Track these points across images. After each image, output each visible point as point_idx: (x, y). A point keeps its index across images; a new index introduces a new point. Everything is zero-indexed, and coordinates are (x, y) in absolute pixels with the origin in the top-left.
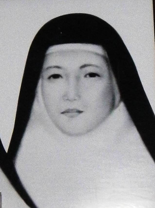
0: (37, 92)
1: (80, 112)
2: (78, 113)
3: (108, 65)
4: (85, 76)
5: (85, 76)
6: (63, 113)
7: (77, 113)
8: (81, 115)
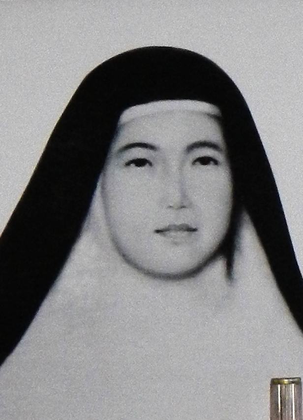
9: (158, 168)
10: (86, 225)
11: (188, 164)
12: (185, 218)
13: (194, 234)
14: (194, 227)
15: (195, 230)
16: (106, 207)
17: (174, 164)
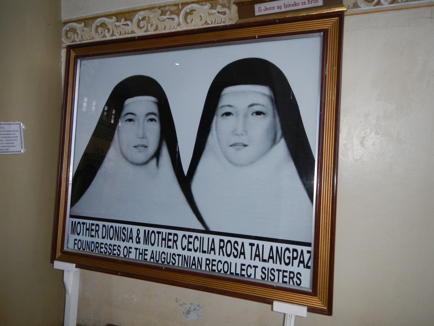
0: (212, 127)
1: (245, 146)
2: (243, 146)
3: (273, 105)
4: (252, 114)
5: (252, 114)
6: (231, 146)
7: (242, 147)
8: (246, 148)
9: (136, 123)
10: (112, 143)
12: (144, 142)
13: (147, 148)
14: (146, 145)
15: (147, 147)
16: (119, 137)
17: (141, 121)
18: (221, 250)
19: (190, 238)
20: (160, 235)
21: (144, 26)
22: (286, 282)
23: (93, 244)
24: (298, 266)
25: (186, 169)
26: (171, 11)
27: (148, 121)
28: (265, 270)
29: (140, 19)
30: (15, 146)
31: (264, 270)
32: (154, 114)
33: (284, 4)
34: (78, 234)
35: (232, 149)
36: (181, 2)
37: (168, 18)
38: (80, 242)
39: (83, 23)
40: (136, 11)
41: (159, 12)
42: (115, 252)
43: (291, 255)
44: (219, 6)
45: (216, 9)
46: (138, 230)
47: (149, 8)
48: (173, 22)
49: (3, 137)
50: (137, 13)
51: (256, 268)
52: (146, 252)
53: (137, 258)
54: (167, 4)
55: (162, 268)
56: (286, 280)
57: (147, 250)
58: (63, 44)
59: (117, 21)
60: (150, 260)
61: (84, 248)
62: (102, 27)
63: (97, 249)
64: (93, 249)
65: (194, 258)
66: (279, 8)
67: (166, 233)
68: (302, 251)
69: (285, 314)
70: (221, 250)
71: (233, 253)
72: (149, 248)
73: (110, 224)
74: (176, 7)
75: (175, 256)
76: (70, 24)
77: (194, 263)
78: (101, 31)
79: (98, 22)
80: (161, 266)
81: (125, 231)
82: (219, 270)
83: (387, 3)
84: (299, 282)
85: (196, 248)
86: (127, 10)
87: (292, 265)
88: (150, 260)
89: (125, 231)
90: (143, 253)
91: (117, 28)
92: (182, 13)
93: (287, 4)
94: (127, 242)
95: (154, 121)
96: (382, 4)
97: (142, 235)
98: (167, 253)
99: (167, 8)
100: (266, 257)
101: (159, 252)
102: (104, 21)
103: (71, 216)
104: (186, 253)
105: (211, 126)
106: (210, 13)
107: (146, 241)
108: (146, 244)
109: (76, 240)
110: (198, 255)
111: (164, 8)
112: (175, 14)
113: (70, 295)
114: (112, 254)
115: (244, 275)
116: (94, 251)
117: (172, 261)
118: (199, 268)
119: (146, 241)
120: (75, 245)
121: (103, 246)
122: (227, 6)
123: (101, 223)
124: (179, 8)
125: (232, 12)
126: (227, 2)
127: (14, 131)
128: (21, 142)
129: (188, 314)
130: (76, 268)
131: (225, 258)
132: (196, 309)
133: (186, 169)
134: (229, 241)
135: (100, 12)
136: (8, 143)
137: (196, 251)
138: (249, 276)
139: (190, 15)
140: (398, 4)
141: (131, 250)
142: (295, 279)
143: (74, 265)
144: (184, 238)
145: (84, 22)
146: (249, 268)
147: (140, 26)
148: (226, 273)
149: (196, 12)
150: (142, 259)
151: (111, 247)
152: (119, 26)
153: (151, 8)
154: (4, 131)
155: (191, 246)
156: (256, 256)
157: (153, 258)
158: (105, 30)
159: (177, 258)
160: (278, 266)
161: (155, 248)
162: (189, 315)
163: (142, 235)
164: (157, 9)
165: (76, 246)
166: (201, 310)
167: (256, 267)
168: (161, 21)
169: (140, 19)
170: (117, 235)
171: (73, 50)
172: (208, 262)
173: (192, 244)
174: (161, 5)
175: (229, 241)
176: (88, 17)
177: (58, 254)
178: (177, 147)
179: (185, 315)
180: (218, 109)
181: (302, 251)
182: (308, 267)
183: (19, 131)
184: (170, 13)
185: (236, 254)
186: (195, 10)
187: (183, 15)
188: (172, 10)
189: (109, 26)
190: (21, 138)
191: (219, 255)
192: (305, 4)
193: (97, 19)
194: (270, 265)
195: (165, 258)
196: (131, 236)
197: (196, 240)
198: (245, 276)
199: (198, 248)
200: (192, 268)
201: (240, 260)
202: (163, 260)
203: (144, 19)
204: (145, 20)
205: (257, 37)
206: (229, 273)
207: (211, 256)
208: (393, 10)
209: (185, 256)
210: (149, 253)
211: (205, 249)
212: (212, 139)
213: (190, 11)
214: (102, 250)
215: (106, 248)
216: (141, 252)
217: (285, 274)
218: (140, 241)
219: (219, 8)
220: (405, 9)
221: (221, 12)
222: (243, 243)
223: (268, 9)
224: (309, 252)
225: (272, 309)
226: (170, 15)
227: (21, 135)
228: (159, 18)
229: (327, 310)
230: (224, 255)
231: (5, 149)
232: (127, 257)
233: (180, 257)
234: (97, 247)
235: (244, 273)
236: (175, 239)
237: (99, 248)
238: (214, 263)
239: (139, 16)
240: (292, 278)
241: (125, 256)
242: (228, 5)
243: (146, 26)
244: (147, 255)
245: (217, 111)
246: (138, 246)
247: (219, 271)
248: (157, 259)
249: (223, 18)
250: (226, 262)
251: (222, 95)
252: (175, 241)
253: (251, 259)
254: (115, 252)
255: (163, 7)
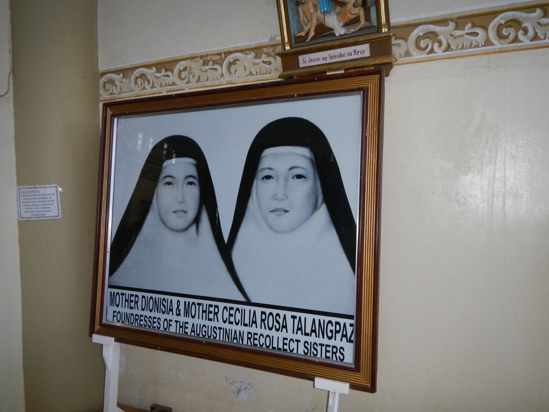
0: (252, 191)
1: (286, 211)
2: (284, 212)
3: (314, 168)
4: (293, 178)
6: (272, 211)
9: (175, 185)
11: (185, 184)
12: (183, 207)
13: (186, 214)
14: (186, 210)
17: (180, 184)
18: (263, 323)
19: (231, 311)
20: (201, 307)
21: (186, 77)
22: (329, 358)
23: (132, 316)
24: (341, 340)
25: (226, 235)
26: (213, 61)
27: (187, 184)
28: (308, 344)
29: (182, 70)
30: (51, 211)
31: (306, 344)
32: (194, 177)
33: (329, 55)
34: (117, 306)
35: (272, 215)
36: (224, 51)
37: (211, 69)
38: (119, 314)
39: (122, 74)
40: (177, 61)
41: (201, 61)
42: (155, 325)
43: (333, 328)
44: (264, 54)
45: (260, 58)
46: (179, 301)
47: (191, 57)
48: (215, 72)
49: (39, 202)
50: (178, 64)
51: (299, 343)
52: (187, 325)
53: (178, 332)
54: (209, 53)
55: (203, 342)
56: (329, 355)
57: (187, 323)
58: (101, 97)
59: (157, 72)
60: (191, 334)
61: (123, 320)
62: (141, 78)
63: (136, 321)
64: (132, 322)
65: (236, 331)
66: (324, 60)
67: (207, 305)
68: (345, 324)
69: (329, 392)
70: (263, 323)
71: (275, 326)
72: (190, 320)
73: (149, 295)
74: (219, 56)
75: (216, 330)
76: (108, 75)
77: (235, 337)
78: (141, 83)
79: (137, 73)
80: (202, 340)
81: (165, 302)
82: (261, 344)
83: (441, 51)
84: (342, 357)
85: (237, 321)
86: (167, 60)
87: (335, 339)
88: (191, 334)
89: (165, 302)
90: (184, 326)
91: (157, 79)
92: (226, 63)
93: (333, 55)
94: (167, 314)
95: (193, 184)
96: (435, 53)
97: (182, 307)
98: (208, 326)
99: (209, 58)
100: (308, 331)
101: (200, 325)
102: (144, 71)
103: (110, 286)
104: (227, 326)
105: (251, 190)
106: (255, 63)
107: (186, 314)
108: (186, 317)
109: (115, 312)
110: (240, 328)
111: (206, 57)
112: (218, 64)
113: (110, 370)
114: (152, 327)
115: (286, 350)
116: (134, 324)
117: (213, 335)
118: (241, 342)
119: (186, 314)
120: (114, 318)
121: (142, 318)
122: (272, 55)
123: (140, 294)
124: (222, 57)
125: (277, 62)
126: (272, 51)
127: (50, 195)
128: (58, 206)
129: (239, 394)
130: (115, 341)
131: (266, 332)
132: (247, 388)
133: (226, 234)
134: (271, 314)
135: (139, 62)
136: (44, 208)
137: (237, 324)
138: (292, 351)
139: (234, 65)
140: (452, 52)
141: (171, 323)
142: (338, 354)
143: (113, 339)
144: (225, 310)
145: (123, 74)
146: (292, 342)
147: (182, 77)
148: (268, 347)
149: (239, 62)
150: (182, 332)
151: (151, 319)
152: (160, 77)
153: (192, 58)
154: (40, 195)
155: (232, 319)
156: (299, 329)
157: (194, 331)
158: (145, 82)
159: (218, 331)
160: (320, 340)
161: (196, 321)
162: (240, 394)
163: (182, 307)
164: (198, 59)
165: (115, 318)
166: (252, 389)
167: (298, 341)
168: (203, 72)
169: (182, 70)
170: (157, 306)
171: (109, 108)
172: (250, 336)
173: (233, 316)
174: (202, 54)
175: (271, 314)
176: (127, 67)
177: (97, 327)
178: (217, 212)
179: (236, 394)
180: (258, 172)
181: (345, 324)
182: (351, 341)
183: (56, 195)
184: (212, 62)
185: (278, 327)
186: (239, 60)
187: (226, 65)
188: (214, 60)
189: (149, 78)
190: (58, 202)
191: (261, 328)
192: (351, 55)
193: (136, 70)
194: (312, 339)
195: (206, 331)
196: (171, 308)
197: (237, 312)
198: (288, 351)
199: (239, 320)
200: (234, 342)
201: (282, 334)
202: (204, 334)
203: (185, 69)
204: (186, 71)
205: (296, 96)
206: (271, 347)
207: (253, 330)
208: (448, 58)
209: (226, 329)
210: (190, 326)
211: (247, 322)
212: (252, 204)
213: (233, 60)
214: (142, 323)
215: (146, 321)
216: (181, 325)
217: (328, 349)
218: (181, 313)
219: (264, 58)
220: (460, 57)
221: (266, 62)
222: (285, 316)
223: (313, 61)
224: (351, 325)
225: (314, 387)
226: (213, 65)
227: (57, 199)
228: (201, 69)
229: (370, 387)
230: (265, 329)
231: (41, 215)
232: (167, 330)
233: (221, 330)
234: (137, 320)
235: (286, 347)
236: (216, 311)
237: (139, 321)
238: (256, 337)
239: (180, 66)
240: (335, 353)
241: (165, 329)
242: (273, 54)
243: (187, 78)
244: (187, 328)
245: (258, 174)
246: (178, 318)
247: (261, 346)
248: (198, 333)
249: (269, 68)
250: (268, 336)
251: (263, 157)
252: (216, 314)
253: (293, 333)
254: (155, 325)
255: (205, 56)
